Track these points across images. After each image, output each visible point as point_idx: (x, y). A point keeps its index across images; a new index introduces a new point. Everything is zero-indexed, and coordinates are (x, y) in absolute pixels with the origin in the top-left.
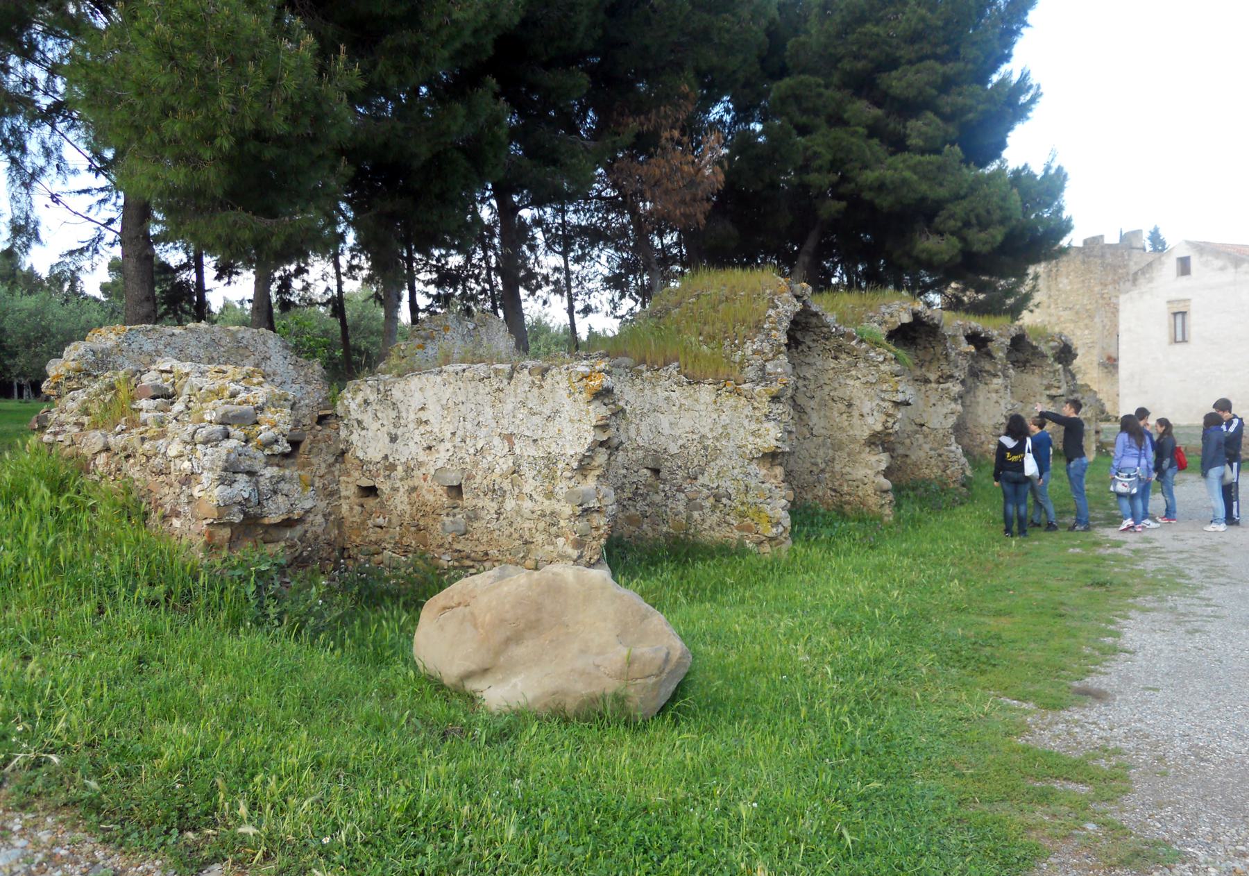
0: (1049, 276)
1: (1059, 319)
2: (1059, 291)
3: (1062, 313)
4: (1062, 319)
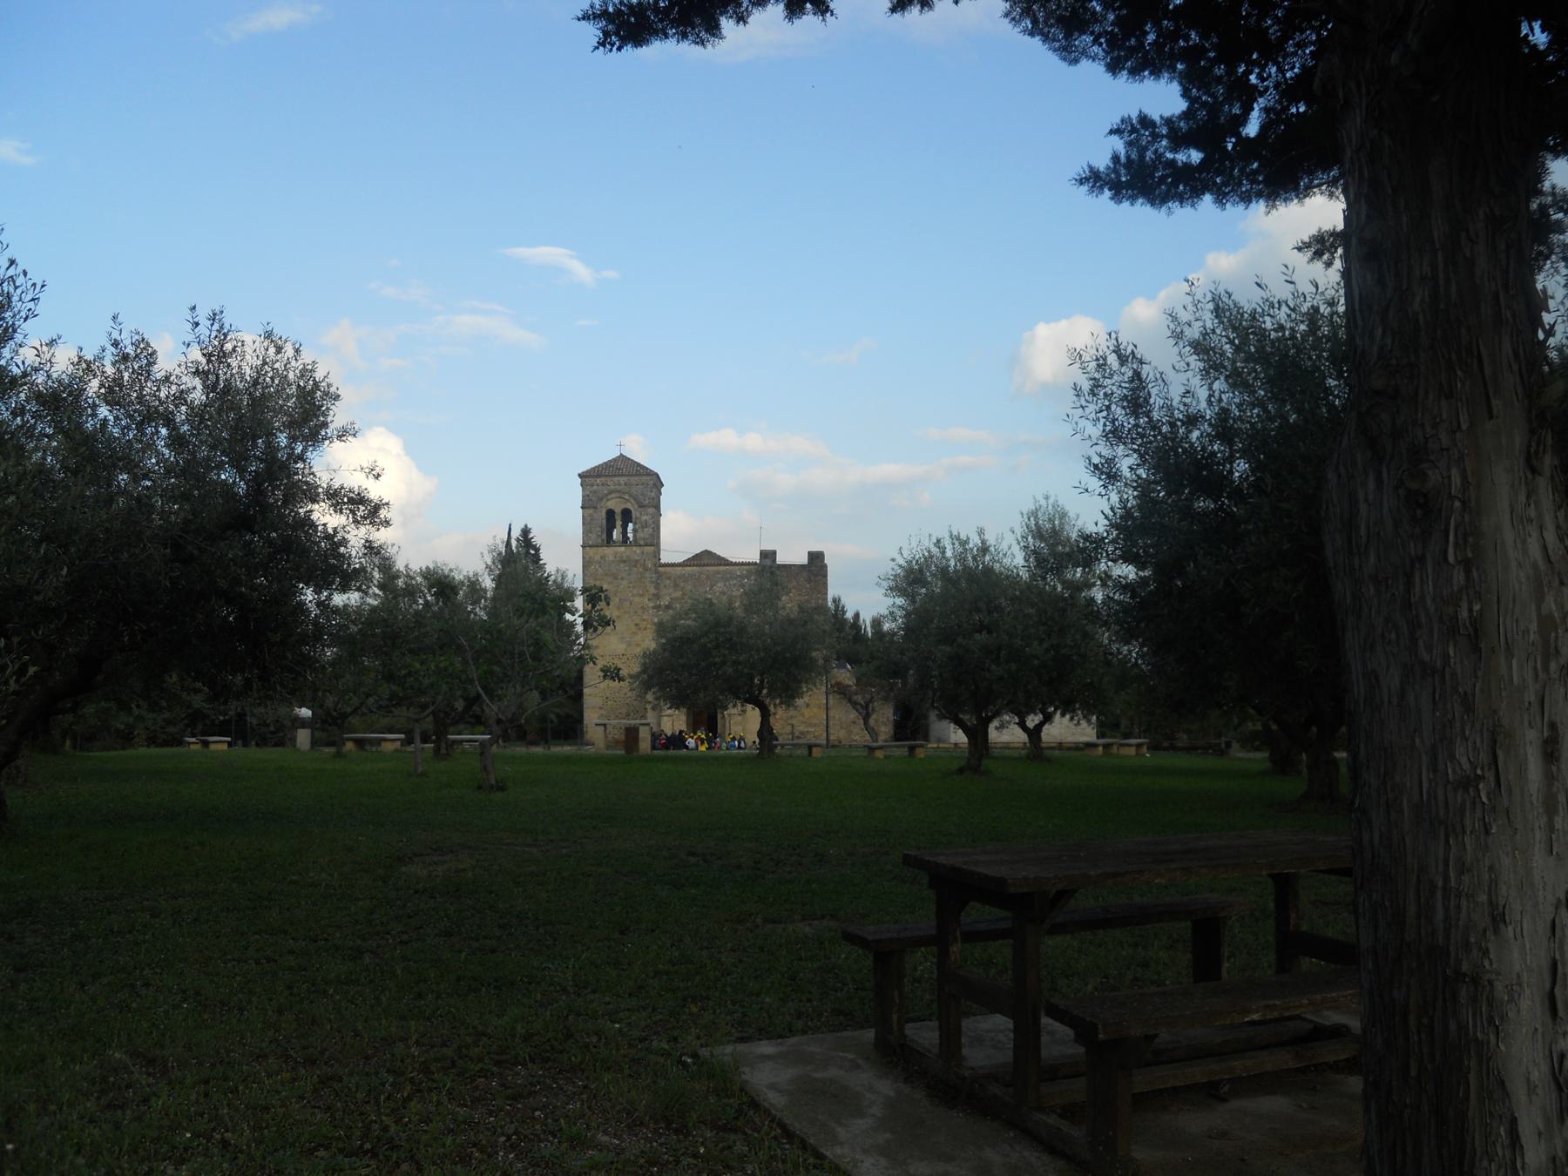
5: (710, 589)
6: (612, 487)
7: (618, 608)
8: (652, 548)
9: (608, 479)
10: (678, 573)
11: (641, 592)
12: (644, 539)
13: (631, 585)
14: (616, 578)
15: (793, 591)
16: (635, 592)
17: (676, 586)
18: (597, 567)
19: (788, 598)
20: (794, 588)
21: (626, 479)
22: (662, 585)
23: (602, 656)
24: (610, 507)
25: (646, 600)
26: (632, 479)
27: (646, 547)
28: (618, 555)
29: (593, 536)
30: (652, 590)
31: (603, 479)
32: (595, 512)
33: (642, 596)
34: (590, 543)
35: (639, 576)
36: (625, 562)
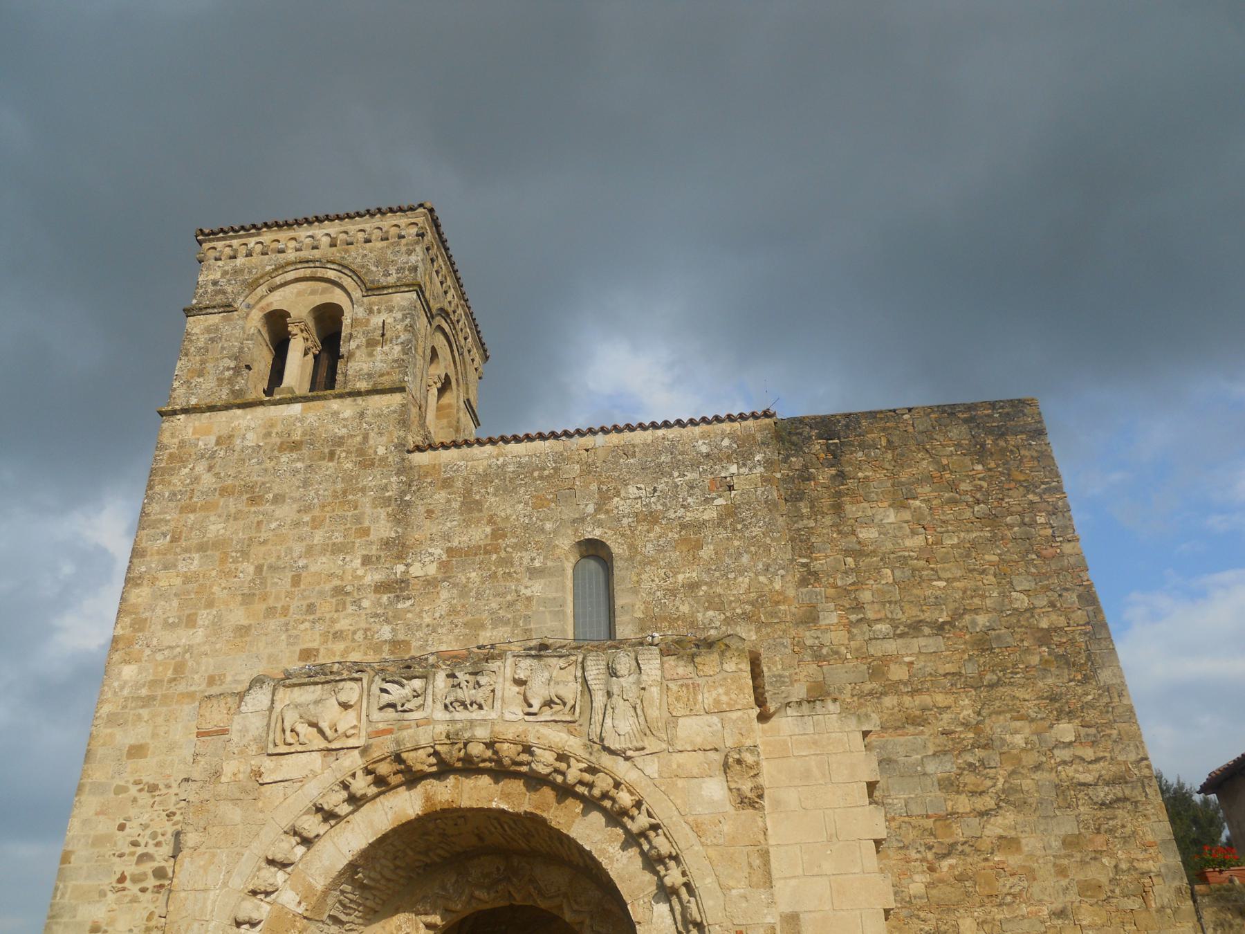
0: (795, 498)
2: (858, 554)
3: (891, 647)
4: (897, 673)
5: (597, 510)
6: (291, 255)
7: (247, 599)
8: (397, 398)
9: (284, 235)
11: (338, 538)
12: (370, 376)
13: (307, 518)
14: (253, 501)
15: (925, 490)
16: (318, 537)
17: (471, 506)
18: (201, 467)
19: (907, 515)
20: (929, 479)
21: (334, 228)
23: (153, 788)
24: (275, 307)
25: (357, 562)
26: (352, 227)
27: (377, 397)
28: (279, 428)
30: (383, 529)
31: (267, 237)
33: (337, 549)
34: (193, 401)
35: (340, 486)
36: (296, 446)
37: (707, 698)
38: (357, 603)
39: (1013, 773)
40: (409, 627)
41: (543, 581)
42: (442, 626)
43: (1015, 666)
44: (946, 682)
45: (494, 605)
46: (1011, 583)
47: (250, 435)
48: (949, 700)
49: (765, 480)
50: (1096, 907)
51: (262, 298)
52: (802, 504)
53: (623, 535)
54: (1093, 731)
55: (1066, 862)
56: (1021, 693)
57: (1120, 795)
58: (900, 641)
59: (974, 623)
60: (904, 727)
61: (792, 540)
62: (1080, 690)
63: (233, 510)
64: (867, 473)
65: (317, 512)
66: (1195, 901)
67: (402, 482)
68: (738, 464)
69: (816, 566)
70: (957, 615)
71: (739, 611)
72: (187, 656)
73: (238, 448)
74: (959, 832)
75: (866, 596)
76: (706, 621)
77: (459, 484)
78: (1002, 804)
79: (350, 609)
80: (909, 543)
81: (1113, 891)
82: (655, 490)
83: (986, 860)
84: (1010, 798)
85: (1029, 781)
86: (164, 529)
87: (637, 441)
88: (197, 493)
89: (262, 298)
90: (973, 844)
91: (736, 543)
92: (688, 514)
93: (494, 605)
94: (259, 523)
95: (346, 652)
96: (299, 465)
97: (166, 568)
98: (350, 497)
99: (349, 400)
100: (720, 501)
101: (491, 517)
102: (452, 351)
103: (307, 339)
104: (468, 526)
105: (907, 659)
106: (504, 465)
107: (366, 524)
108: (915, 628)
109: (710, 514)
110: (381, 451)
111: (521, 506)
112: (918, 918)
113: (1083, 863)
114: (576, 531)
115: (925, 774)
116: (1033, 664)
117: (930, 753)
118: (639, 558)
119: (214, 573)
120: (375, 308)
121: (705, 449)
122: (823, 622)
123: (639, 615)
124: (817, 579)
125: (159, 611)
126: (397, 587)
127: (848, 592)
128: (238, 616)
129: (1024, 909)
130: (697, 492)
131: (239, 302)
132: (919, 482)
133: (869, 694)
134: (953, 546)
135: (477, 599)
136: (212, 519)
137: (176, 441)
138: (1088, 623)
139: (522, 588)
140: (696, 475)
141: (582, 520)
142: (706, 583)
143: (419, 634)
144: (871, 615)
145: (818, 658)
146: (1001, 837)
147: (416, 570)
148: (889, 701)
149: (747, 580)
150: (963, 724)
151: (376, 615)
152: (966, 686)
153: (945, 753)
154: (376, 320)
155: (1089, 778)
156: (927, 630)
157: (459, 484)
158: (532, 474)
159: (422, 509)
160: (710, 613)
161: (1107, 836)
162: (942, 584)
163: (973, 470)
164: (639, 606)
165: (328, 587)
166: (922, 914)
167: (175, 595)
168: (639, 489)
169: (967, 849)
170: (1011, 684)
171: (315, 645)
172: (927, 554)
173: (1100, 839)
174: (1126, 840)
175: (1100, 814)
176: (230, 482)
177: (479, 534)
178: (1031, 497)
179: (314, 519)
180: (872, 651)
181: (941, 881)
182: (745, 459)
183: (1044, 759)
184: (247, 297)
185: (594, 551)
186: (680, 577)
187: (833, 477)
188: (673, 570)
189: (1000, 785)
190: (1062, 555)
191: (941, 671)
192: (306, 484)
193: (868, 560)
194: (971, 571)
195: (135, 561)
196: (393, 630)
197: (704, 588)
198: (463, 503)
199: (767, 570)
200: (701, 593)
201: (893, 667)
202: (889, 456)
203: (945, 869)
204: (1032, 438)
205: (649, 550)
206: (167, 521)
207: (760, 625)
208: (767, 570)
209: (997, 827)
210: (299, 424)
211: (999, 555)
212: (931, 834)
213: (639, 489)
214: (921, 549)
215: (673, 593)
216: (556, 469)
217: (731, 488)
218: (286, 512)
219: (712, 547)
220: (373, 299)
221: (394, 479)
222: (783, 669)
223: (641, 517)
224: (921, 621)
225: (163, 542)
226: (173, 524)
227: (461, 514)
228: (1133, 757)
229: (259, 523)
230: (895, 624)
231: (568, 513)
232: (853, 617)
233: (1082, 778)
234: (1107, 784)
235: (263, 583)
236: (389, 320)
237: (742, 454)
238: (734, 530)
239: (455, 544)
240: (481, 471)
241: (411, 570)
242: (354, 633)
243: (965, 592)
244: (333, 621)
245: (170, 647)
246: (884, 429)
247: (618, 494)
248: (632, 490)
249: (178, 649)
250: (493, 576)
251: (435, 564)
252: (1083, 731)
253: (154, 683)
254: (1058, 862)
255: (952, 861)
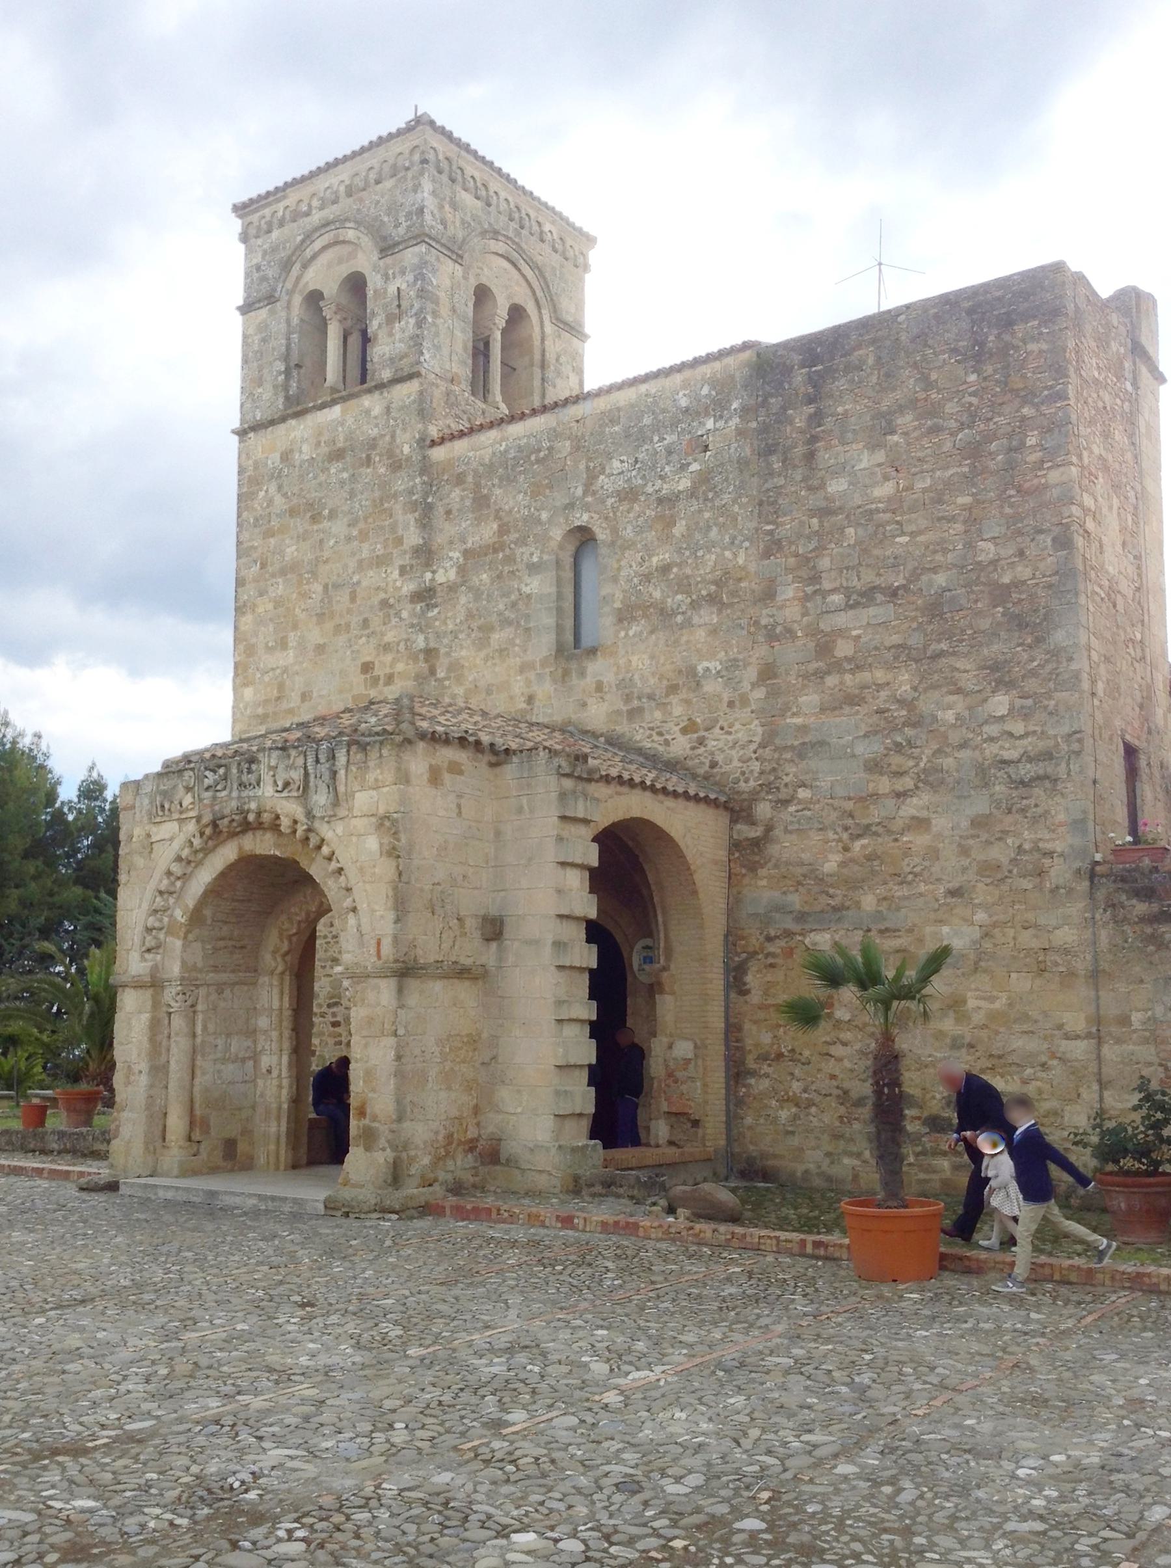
1: (824, 649)
3: (841, 620)
4: (844, 649)
5: (585, 493)
6: (316, 217)
8: (413, 386)
10: (486, 454)
11: (380, 549)
14: (315, 519)
17: (481, 502)
18: (273, 488)
19: (880, 456)
22: (440, 510)
24: (311, 287)
27: (399, 387)
29: (266, 393)
30: (413, 538)
32: (272, 312)
33: (381, 561)
35: (377, 494)
36: (337, 455)
37: (371, 777)
38: (398, 614)
39: (938, 752)
40: (438, 636)
41: (539, 577)
42: (462, 632)
43: (963, 631)
44: (889, 656)
45: (501, 607)
46: (980, 530)
47: (305, 448)
48: (890, 676)
49: (740, 433)
50: (991, 888)
51: (298, 279)
52: (774, 458)
53: (606, 518)
54: (1029, 702)
55: (971, 842)
56: (960, 664)
57: (1041, 772)
58: (851, 613)
59: (930, 584)
60: (841, 708)
61: (761, 504)
62: (1025, 656)
63: (301, 530)
64: (847, 407)
65: (361, 525)
66: (1092, 882)
67: (424, 483)
68: (715, 416)
69: (782, 532)
70: (915, 576)
71: (704, 593)
72: (285, 676)
73: (297, 463)
74: (875, 814)
75: (825, 563)
76: (675, 606)
77: (470, 479)
78: (921, 785)
79: (394, 621)
80: (878, 492)
81: (1010, 871)
82: (636, 462)
83: (896, 840)
84: (930, 779)
85: (950, 760)
86: (255, 555)
87: (622, 403)
88: (273, 517)
89: (298, 279)
90: (885, 826)
91: (707, 515)
92: (665, 486)
93: (501, 607)
94: (321, 541)
95: (393, 664)
96: (345, 475)
97: (261, 595)
98: (386, 505)
99: (377, 395)
100: (695, 467)
101: (497, 511)
102: (519, 270)
103: (345, 319)
104: (478, 525)
105: (854, 633)
106: (506, 451)
107: (400, 532)
108: (868, 595)
109: (685, 484)
110: (406, 449)
111: (521, 496)
112: (828, 894)
113: (988, 843)
114: (567, 519)
115: (854, 756)
116: (982, 628)
117: (862, 734)
118: (619, 542)
119: (295, 596)
120: (390, 272)
121: (684, 402)
122: (780, 598)
123: (618, 605)
124: (780, 548)
125: (261, 637)
126: (425, 596)
127: (808, 560)
128: (315, 636)
129: (922, 888)
130: (675, 457)
131: (279, 290)
132: (901, 409)
133: (813, 675)
134: (924, 491)
135: (488, 602)
136: (287, 542)
137: (251, 462)
138: (1057, 573)
139: (523, 585)
140: (674, 437)
141: (571, 506)
142: (677, 565)
143: (445, 641)
144: (827, 585)
145: (772, 637)
146: (913, 818)
147: (441, 578)
148: (831, 681)
149: (713, 557)
150: (898, 701)
151: (412, 626)
152: (910, 658)
153: (876, 733)
154: (392, 289)
155: (1013, 754)
156: (880, 597)
157: (470, 479)
158: (529, 458)
159: (441, 509)
160: (679, 597)
161: (1017, 816)
162: (906, 539)
163: (965, 382)
164: (619, 595)
165: (376, 601)
166: (831, 891)
167: (271, 620)
168: (622, 462)
169: (880, 830)
170: (954, 654)
171: (368, 659)
172: (895, 504)
173: (1009, 819)
174: (1035, 820)
175: (1015, 793)
176: (295, 501)
177: (488, 532)
178: (1026, 411)
179: (361, 532)
180: (822, 626)
181: (852, 860)
182: (723, 408)
183: (971, 736)
184: (284, 282)
185: (583, 538)
186: (655, 560)
187: (811, 417)
188: (649, 552)
189: (922, 765)
190: (1046, 487)
191: (887, 644)
192: (352, 494)
193: (834, 519)
194: (939, 519)
195: (239, 590)
196: (426, 638)
197: (675, 570)
198: (474, 500)
199: (733, 543)
200: (672, 576)
201: (840, 642)
202: (874, 379)
203: (858, 849)
204: (1045, 323)
205: (629, 533)
206: (256, 548)
207: (722, 606)
208: (733, 543)
209: (912, 808)
210: (340, 429)
211: (973, 495)
212: (851, 815)
213: (622, 462)
214: (890, 500)
215: (647, 578)
216: (550, 449)
217: (706, 448)
218: (338, 527)
219: (684, 523)
220: (389, 260)
221: (418, 480)
222: (739, 653)
223: (622, 496)
224: (874, 588)
225: (256, 569)
226: (260, 550)
227: (473, 512)
228: (1066, 729)
229: (321, 541)
230: (848, 592)
231: (560, 499)
232: (809, 589)
233: (1007, 755)
234: (1030, 760)
235: (330, 602)
236: (404, 286)
237: (718, 407)
238: (706, 499)
239: (469, 545)
240: (487, 461)
241: (437, 577)
242: (398, 644)
243: (927, 547)
244: (383, 634)
245: (273, 669)
246: (874, 341)
247: (603, 471)
248: (616, 464)
249: (278, 671)
250: (499, 577)
251: (454, 569)
252: (1019, 702)
253: (266, 701)
254: (963, 842)
255: (864, 841)
